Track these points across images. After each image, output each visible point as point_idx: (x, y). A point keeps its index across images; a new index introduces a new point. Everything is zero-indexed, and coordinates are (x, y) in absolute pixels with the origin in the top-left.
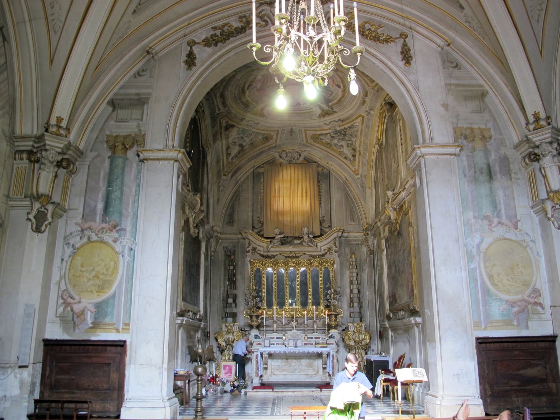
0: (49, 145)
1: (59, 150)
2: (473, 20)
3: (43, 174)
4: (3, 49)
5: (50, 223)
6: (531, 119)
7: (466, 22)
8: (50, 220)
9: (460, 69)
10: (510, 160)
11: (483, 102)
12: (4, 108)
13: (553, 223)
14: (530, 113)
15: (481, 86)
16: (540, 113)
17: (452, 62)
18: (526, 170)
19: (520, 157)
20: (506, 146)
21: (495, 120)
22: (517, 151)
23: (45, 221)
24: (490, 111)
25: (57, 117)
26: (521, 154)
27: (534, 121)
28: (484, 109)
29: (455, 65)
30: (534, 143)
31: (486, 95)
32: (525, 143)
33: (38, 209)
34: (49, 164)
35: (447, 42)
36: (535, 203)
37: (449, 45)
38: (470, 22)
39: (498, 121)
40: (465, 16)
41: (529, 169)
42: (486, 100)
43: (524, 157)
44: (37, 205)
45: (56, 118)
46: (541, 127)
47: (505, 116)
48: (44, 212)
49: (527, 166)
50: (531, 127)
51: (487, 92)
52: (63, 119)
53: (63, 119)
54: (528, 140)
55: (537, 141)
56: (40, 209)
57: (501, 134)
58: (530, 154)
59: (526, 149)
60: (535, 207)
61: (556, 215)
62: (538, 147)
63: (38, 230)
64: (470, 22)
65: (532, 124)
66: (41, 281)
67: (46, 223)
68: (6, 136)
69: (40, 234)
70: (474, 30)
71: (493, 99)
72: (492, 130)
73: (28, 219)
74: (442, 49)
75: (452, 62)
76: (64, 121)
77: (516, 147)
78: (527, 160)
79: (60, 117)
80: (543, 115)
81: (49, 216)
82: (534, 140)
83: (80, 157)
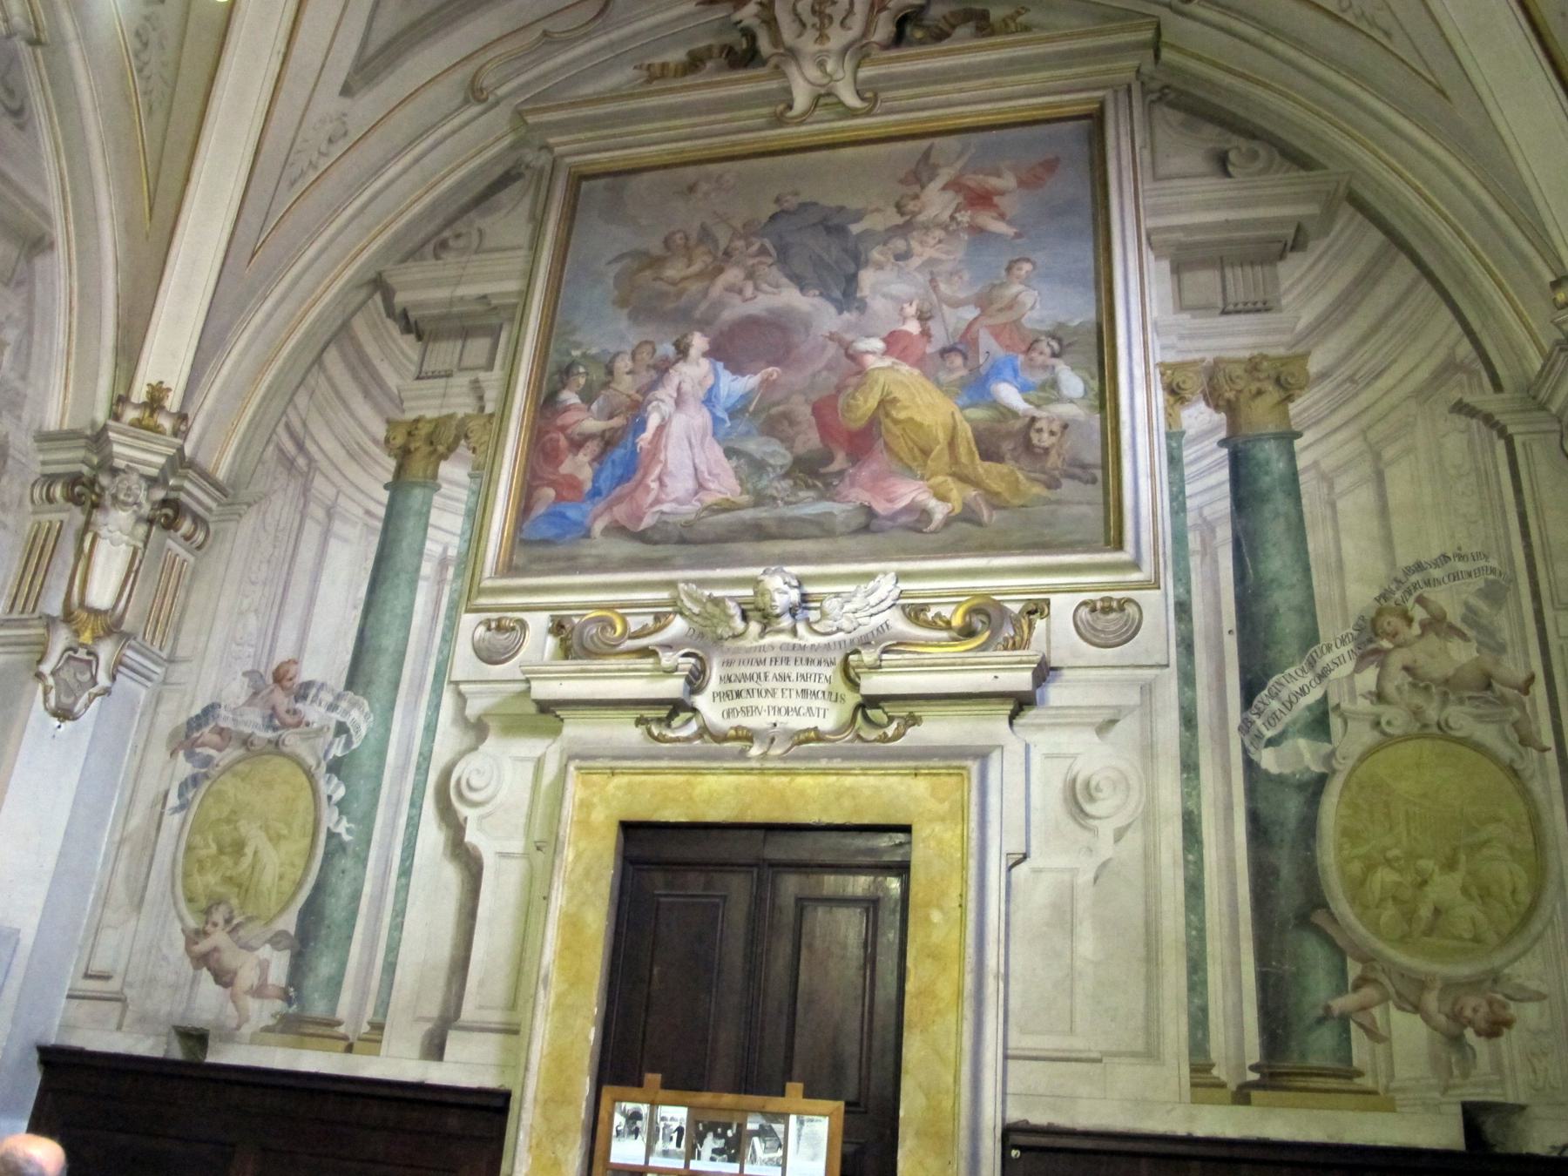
2: (162, 47)
6: (140, 394)
7: (138, 34)
9: (21, 127)
10: (10, 462)
11: (29, 261)
13: (46, 693)
14: (147, 374)
15: (46, 216)
16: (171, 394)
17: (11, 92)
18: (35, 513)
19: (39, 469)
20: (19, 418)
21: (29, 331)
22: (41, 450)
24: (30, 300)
26: (44, 463)
27: (144, 405)
28: (20, 284)
29: (15, 105)
30: (111, 456)
31: (43, 251)
32: (82, 442)
35: (37, 28)
36: (15, 615)
37: (35, 42)
38: (146, 45)
39: (36, 337)
40: (147, 18)
41: (45, 518)
42: (40, 263)
43: (50, 479)
46: (156, 429)
47: (61, 340)
49: (47, 506)
50: (131, 414)
51: (52, 246)
54: (98, 439)
55: (123, 457)
57: (24, 377)
58: (74, 480)
59: (72, 459)
60: (9, 627)
61: (64, 674)
62: (115, 472)
64: (146, 45)
65: (137, 406)
70: (140, 71)
71: (58, 268)
72: (8, 352)
74: (9, 36)
75: (11, 92)
77: (46, 438)
78: (58, 491)
80: (173, 402)
82: (116, 448)
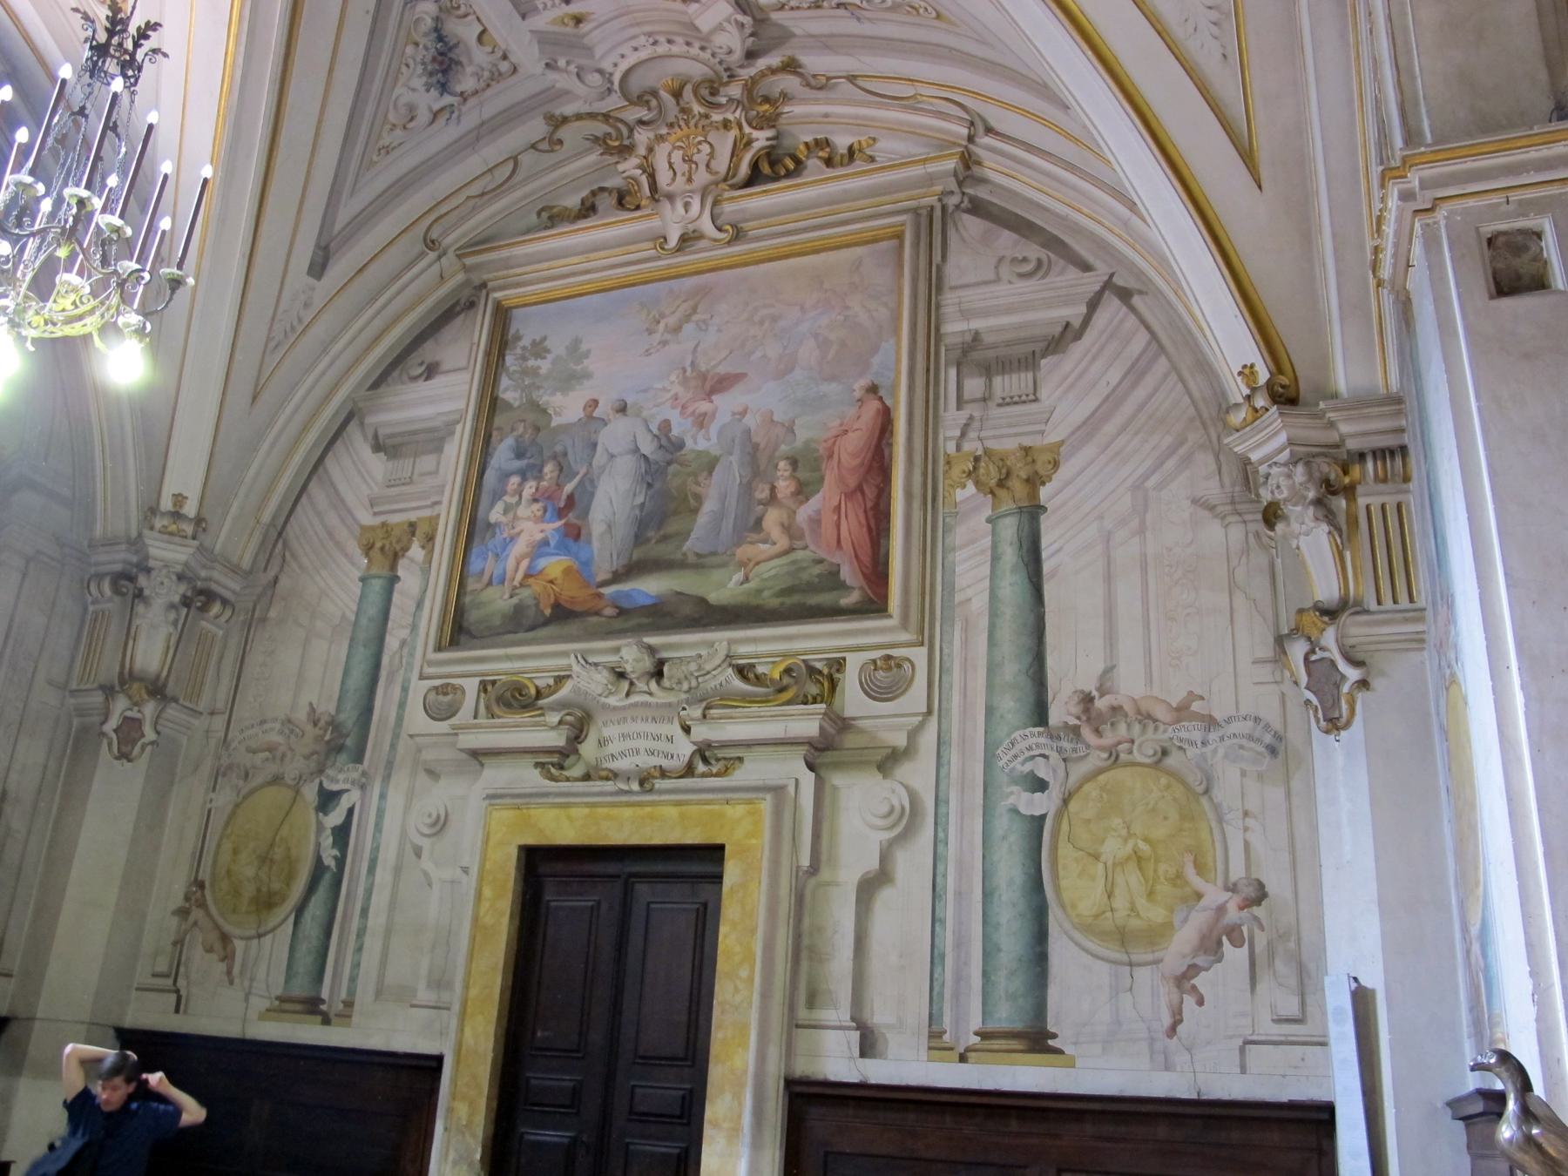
0: (1261, 462)
1: (1286, 455)
3: (1304, 542)
4: (1132, 318)
5: (1363, 684)
8: (1353, 674)
12: (1181, 442)
23: (1338, 686)
25: (1240, 373)
33: (1306, 659)
34: (1299, 508)
44: (1298, 650)
45: (1239, 379)
48: (1322, 659)
52: (1252, 366)
53: (1252, 366)
56: (1313, 658)
63: (1334, 725)
66: (1373, 887)
67: (1345, 689)
68: (1212, 508)
69: (1343, 733)
73: (1308, 702)
76: (1257, 368)
79: (1245, 367)
81: (1342, 666)
83: (1399, 413)
